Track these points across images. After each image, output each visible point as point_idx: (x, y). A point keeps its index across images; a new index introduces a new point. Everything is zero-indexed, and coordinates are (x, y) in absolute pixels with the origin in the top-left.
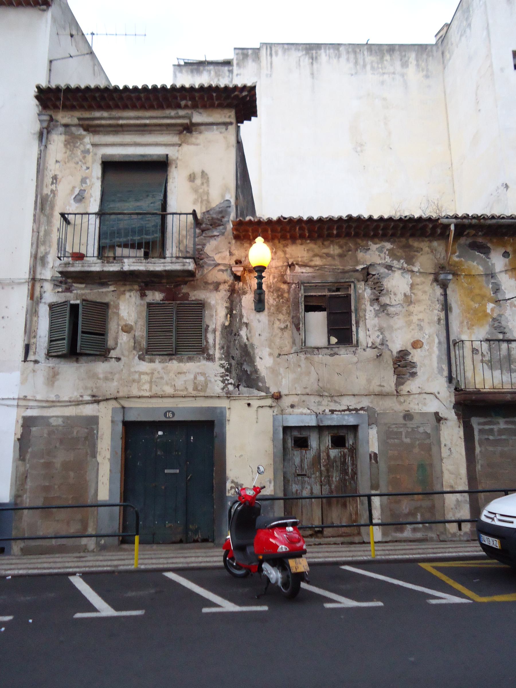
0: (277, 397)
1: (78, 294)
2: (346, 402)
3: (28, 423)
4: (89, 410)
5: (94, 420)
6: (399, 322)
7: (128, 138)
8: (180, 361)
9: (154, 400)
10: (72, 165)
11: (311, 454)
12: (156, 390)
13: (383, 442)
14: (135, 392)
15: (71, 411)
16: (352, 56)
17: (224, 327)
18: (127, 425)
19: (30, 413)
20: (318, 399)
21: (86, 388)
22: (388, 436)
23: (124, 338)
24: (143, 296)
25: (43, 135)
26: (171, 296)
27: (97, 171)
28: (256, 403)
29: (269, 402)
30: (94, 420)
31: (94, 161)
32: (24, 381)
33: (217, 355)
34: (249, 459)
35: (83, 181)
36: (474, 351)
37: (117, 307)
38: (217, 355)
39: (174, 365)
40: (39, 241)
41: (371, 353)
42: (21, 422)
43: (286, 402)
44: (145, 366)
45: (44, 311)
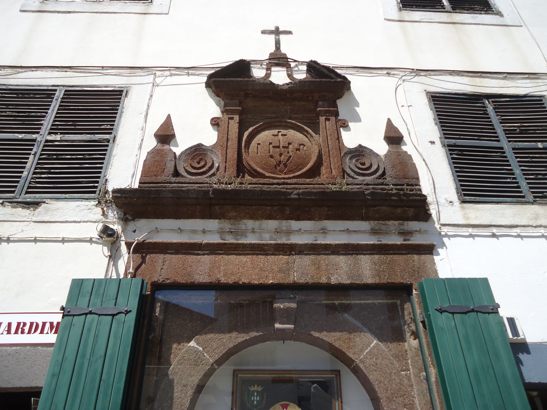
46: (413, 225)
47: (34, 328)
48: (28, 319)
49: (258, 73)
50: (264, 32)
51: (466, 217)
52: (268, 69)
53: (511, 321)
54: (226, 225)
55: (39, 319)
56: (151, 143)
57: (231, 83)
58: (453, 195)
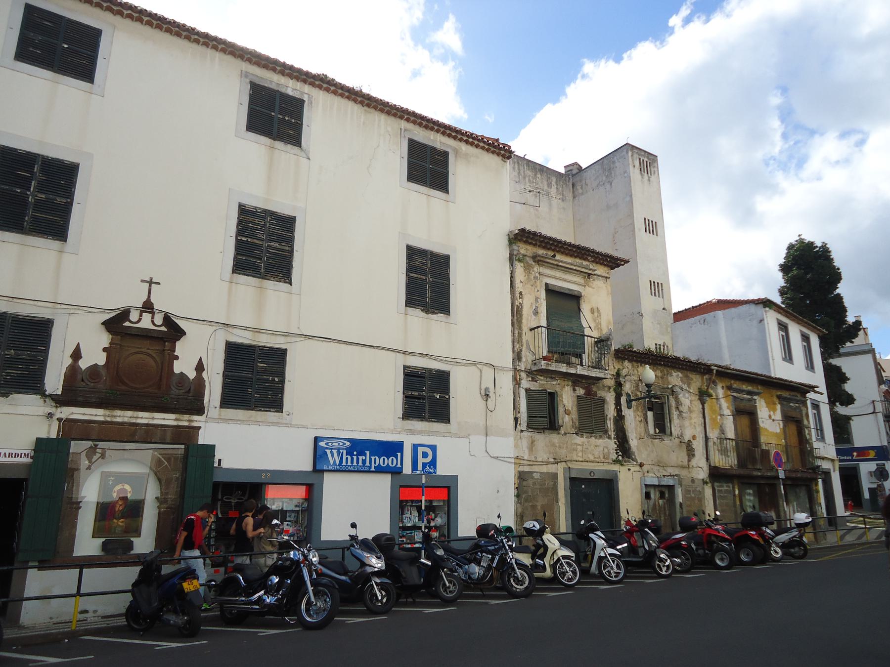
0: (641, 465)
1: (542, 384)
2: (671, 471)
3: (522, 477)
4: (552, 469)
5: (555, 476)
6: (687, 423)
7: (558, 274)
8: (596, 438)
9: (584, 464)
10: (529, 286)
11: (651, 502)
12: (585, 457)
13: (684, 497)
14: (575, 458)
15: (544, 469)
16: (516, 166)
17: (615, 417)
18: (572, 480)
19: (521, 469)
20: (658, 468)
21: (550, 453)
22: (686, 492)
23: (567, 418)
24: (574, 390)
25: (512, 259)
26: (589, 392)
27: (543, 294)
28: (633, 469)
29: (638, 468)
30: (555, 476)
31: (541, 287)
32: (516, 446)
33: (613, 436)
34: (630, 505)
35: (537, 299)
36: (714, 443)
37: (561, 396)
38: (613, 436)
39: (593, 440)
40: (517, 339)
41: (677, 441)
42: (517, 475)
43: (645, 468)
44: (578, 440)
45: (523, 393)
46: (195, 418)
47: (16, 455)
48: (14, 452)
49: (134, 316)
50: (142, 281)
51: (220, 415)
52: (141, 315)
53: (220, 460)
54: (107, 412)
55: (19, 452)
56: (69, 361)
57: (116, 324)
58: (218, 404)
